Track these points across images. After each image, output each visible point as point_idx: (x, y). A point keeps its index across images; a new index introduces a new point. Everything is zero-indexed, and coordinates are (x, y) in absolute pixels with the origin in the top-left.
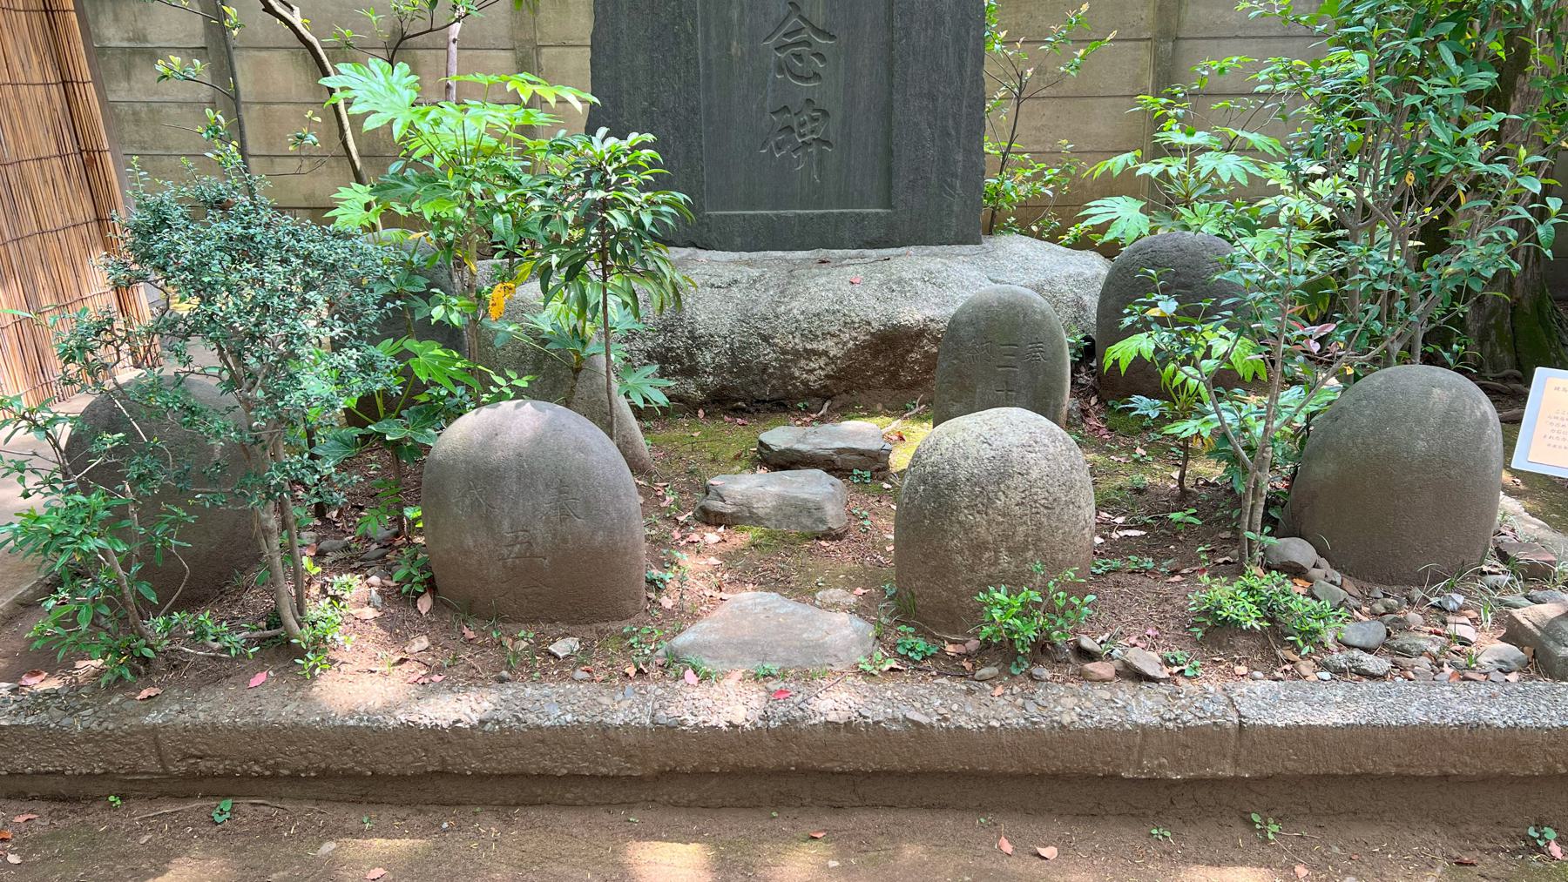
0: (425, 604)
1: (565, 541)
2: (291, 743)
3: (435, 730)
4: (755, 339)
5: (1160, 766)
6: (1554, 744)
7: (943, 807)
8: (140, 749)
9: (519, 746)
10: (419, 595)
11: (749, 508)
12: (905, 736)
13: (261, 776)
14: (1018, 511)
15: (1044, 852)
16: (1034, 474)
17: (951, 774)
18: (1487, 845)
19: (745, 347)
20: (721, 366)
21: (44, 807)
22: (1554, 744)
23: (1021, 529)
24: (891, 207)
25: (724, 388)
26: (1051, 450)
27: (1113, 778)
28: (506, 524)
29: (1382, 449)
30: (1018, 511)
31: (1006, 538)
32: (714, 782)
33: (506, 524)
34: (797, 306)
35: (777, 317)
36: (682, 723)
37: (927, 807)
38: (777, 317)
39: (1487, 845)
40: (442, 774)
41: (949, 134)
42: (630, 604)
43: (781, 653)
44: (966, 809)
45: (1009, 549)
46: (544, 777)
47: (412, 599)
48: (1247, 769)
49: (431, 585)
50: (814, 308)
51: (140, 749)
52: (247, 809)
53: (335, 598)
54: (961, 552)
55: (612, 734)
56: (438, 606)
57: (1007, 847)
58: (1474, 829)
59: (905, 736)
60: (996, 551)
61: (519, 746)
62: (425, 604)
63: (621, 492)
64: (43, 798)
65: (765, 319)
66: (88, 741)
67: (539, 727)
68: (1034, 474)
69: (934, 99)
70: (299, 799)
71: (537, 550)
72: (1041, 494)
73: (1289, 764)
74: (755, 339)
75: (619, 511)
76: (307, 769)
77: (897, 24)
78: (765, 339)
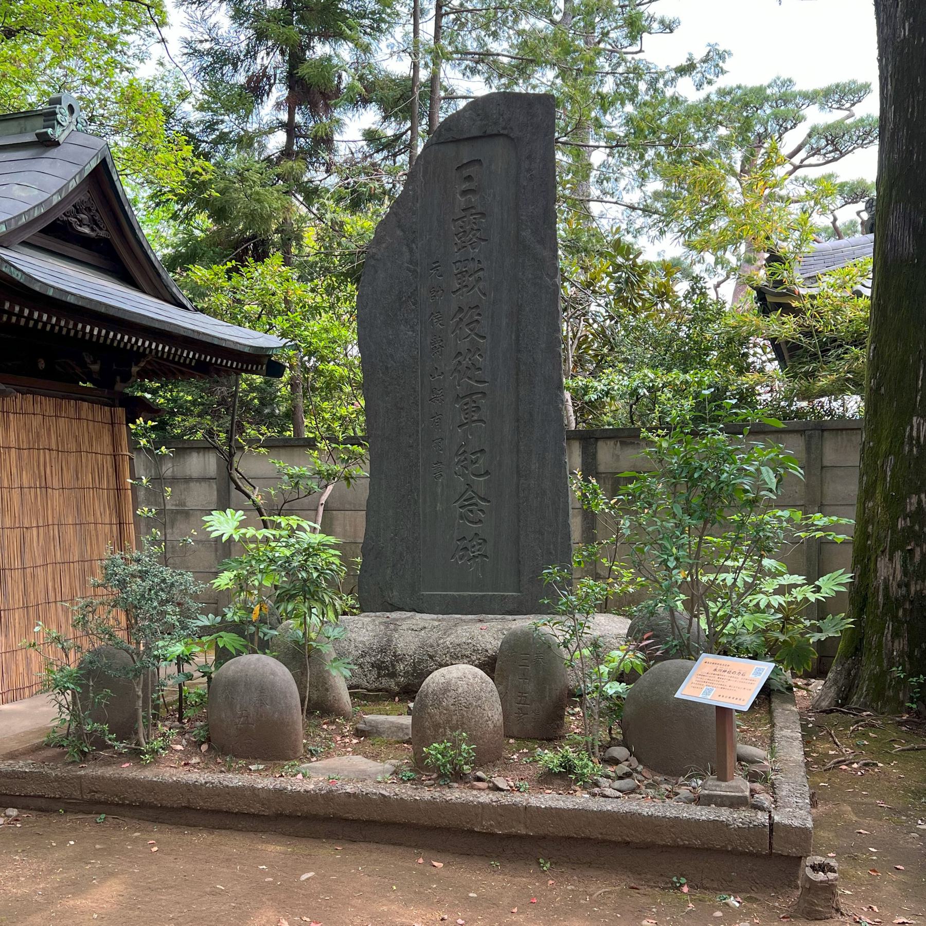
0: (204, 747)
1: (261, 716)
2: (131, 787)
3: (187, 785)
4: (426, 657)
5: (491, 825)
6: (672, 827)
7: (400, 845)
8: (74, 787)
9: (218, 795)
10: (203, 743)
11: (376, 727)
12: (379, 802)
13: (118, 804)
14: (453, 708)
15: (435, 864)
16: (460, 690)
17: (400, 824)
18: (652, 884)
19: (421, 661)
20: (408, 672)
21: (34, 813)
22: (672, 827)
23: (454, 717)
24: (520, 592)
25: (409, 684)
26: (471, 681)
27: (471, 832)
28: (238, 707)
29: (654, 698)
30: (453, 708)
31: (448, 722)
32: (301, 823)
33: (238, 707)
34: (448, 641)
35: (438, 645)
36: (285, 789)
37: (393, 844)
38: (438, 645)
39: (652, 884)
40: (187, 808)
41: (551, 553)
42: (291, 753)
43: (346, 773)
44: (410, 846)
45: (450, 727)
46: (228, 813)
47: (199, 744)
48: (531, 831)
49: (208, 740)
50: (457, 641)
51: (74, 787)
52: (111, 820)
53: (124, 668)
54: (429, 729)
55: (256, 792)
56: (210, 748)
57: (421, 861)
58: (649, 876)
59: (379, 802)
60: (445, 729)
61: (218, 795)
62: (204, 747)
63: (288, 695)
64: (35, 810)
65: (432, 646)
66: (56, 781)
67: (227, 786)
68: (460, 690)
69: (543, 534)
70: (132, 818)
71: (250, 720)
72: (463, 700)
73: (550, 829)
74: (426, 657)
75: (286, 703)
76: (135, 802)
77: (521, 495)
78: (431, 657)
